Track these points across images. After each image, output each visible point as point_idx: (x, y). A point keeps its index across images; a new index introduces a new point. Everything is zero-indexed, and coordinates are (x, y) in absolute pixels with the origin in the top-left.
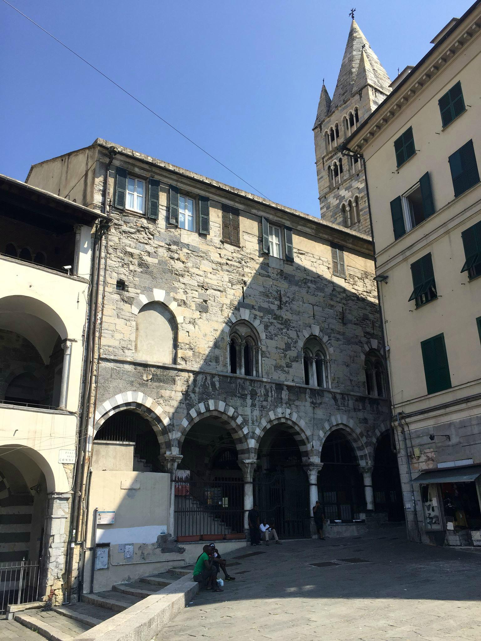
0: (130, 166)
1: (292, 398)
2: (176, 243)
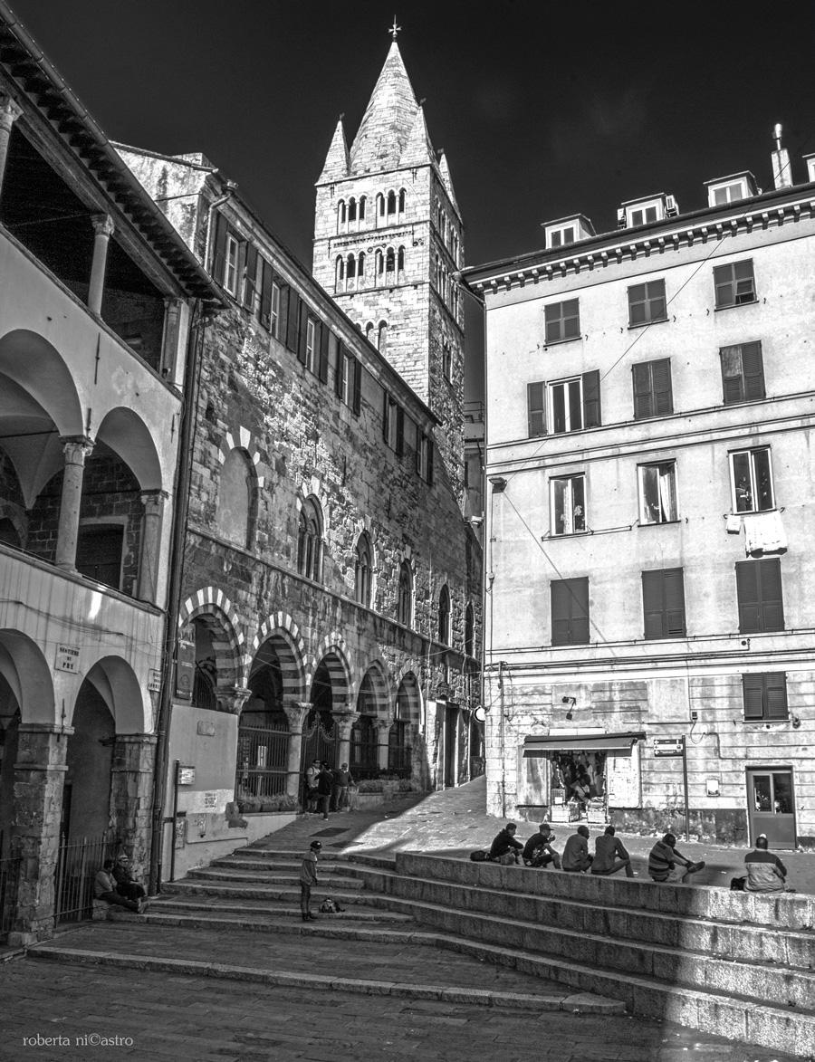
0: (233, 216)
1: (345, 619)
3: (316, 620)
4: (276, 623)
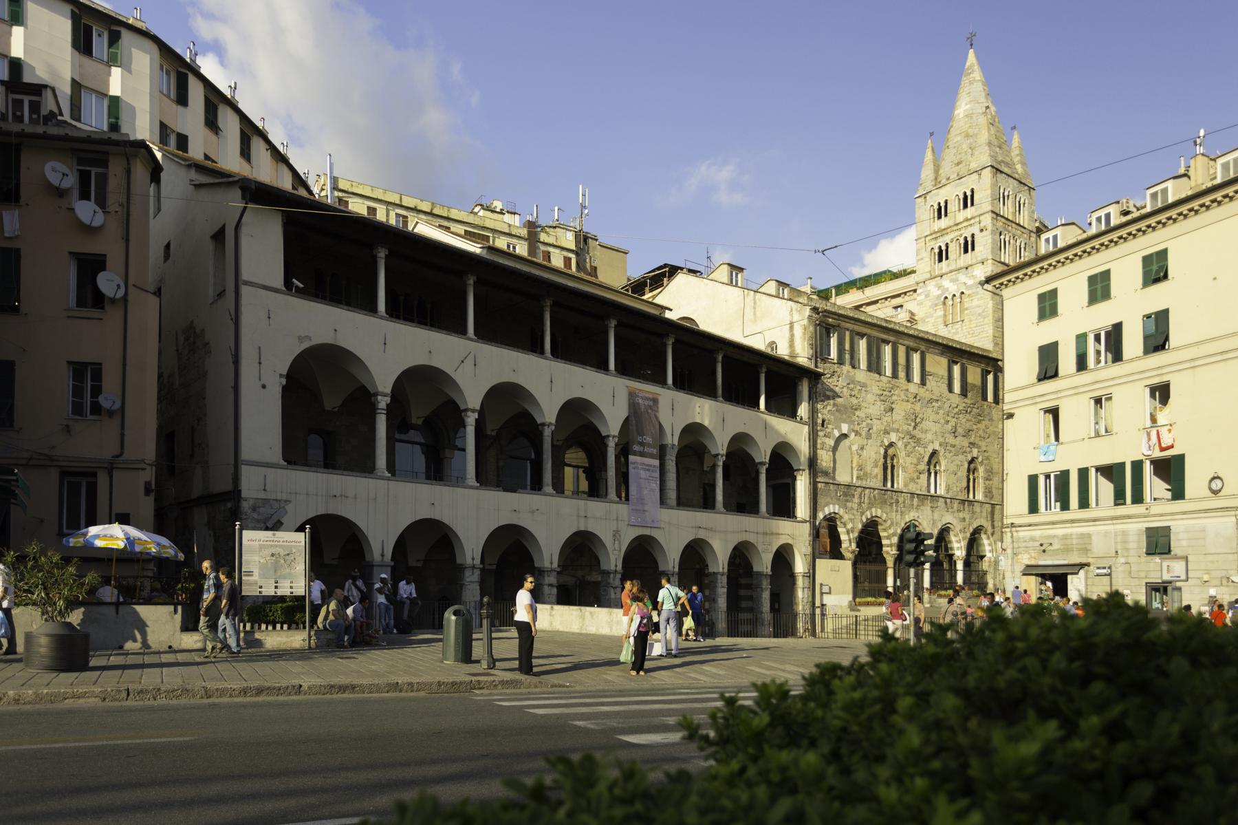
2: (853, 382)
3: (899, 509)
4: (871, 514)
